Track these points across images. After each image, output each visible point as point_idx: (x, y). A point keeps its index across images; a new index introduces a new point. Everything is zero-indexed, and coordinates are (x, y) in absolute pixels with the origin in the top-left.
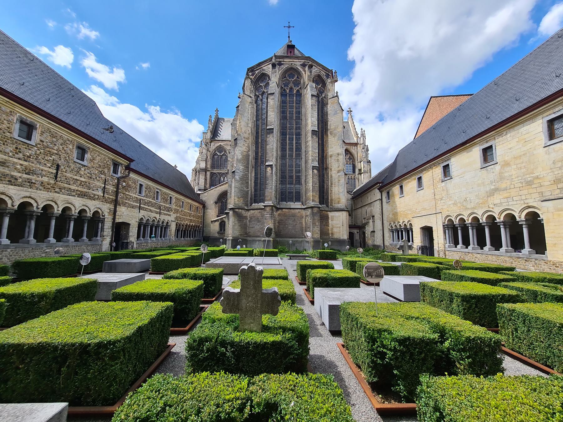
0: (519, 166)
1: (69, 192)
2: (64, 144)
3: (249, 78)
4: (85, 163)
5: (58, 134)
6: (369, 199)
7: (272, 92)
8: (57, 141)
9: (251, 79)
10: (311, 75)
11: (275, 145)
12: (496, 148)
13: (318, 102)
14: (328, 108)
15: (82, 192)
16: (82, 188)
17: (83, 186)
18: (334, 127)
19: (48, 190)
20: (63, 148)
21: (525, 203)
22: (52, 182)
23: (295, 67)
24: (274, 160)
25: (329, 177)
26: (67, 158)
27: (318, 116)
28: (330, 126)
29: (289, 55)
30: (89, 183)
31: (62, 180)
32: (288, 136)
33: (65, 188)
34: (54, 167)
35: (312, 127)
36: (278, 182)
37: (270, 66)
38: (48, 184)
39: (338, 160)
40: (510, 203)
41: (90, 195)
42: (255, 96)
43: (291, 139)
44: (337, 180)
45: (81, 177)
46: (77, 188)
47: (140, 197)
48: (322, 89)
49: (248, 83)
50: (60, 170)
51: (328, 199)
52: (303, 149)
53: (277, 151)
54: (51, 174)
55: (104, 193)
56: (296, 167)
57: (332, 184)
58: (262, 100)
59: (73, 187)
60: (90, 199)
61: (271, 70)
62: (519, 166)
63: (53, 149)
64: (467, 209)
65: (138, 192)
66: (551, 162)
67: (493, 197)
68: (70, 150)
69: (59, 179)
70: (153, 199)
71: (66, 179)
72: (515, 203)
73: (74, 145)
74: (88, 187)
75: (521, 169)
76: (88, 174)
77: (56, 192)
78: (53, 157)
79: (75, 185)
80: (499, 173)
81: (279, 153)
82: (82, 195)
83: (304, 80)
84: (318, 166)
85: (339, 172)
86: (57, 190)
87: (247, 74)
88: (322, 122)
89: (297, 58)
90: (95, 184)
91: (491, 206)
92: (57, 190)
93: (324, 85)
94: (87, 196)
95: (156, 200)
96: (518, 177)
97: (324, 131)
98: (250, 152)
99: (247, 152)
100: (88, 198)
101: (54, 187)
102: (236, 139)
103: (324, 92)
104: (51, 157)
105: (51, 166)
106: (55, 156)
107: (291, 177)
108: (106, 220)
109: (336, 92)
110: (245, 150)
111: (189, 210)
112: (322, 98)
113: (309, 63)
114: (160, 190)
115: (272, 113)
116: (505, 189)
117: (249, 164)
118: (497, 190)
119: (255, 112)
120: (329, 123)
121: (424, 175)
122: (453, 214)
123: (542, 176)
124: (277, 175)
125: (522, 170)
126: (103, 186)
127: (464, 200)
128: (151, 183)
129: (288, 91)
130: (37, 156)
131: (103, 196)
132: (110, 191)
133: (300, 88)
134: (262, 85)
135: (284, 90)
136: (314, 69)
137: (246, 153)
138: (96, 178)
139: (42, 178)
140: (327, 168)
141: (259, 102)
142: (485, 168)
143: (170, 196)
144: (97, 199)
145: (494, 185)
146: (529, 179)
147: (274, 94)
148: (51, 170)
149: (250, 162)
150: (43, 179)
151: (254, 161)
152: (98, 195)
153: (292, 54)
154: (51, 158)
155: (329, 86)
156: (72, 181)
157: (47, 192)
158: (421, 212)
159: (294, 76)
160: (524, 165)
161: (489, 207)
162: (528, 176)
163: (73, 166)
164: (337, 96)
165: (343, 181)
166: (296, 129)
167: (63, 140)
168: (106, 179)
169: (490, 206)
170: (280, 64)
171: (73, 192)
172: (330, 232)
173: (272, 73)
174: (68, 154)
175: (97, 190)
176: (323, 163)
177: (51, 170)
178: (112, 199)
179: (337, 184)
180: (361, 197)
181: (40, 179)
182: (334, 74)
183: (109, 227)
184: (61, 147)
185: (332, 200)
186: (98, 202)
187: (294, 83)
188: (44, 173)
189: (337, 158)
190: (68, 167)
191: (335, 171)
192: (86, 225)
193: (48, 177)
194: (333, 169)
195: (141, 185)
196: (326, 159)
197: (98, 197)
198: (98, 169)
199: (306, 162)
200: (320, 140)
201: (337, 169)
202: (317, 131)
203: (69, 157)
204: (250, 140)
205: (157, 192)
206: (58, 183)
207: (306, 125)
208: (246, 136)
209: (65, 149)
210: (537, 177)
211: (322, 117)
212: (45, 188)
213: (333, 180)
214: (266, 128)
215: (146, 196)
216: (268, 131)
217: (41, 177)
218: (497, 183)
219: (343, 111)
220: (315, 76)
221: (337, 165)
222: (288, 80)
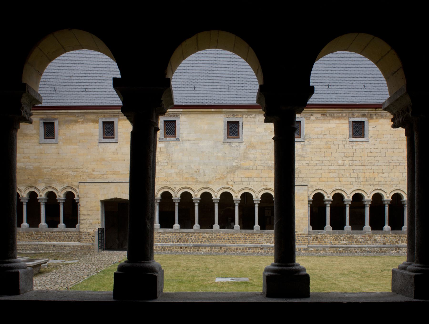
12: (243, 126)
21: (264, 185)
40: (251, 183)
67: (234, 175)
72: (255, 183)
80: (244, 153)
91: (231, 183)
96: (261, 160)
116: (248, 169)
118: (238, 167)
121: (121, 122)
122: (175, 186)
125: (266, 156)
127: (196, 171)
158: (105, 176)
161: (227, 184)
169: (228, 183)
218: (240, 161)
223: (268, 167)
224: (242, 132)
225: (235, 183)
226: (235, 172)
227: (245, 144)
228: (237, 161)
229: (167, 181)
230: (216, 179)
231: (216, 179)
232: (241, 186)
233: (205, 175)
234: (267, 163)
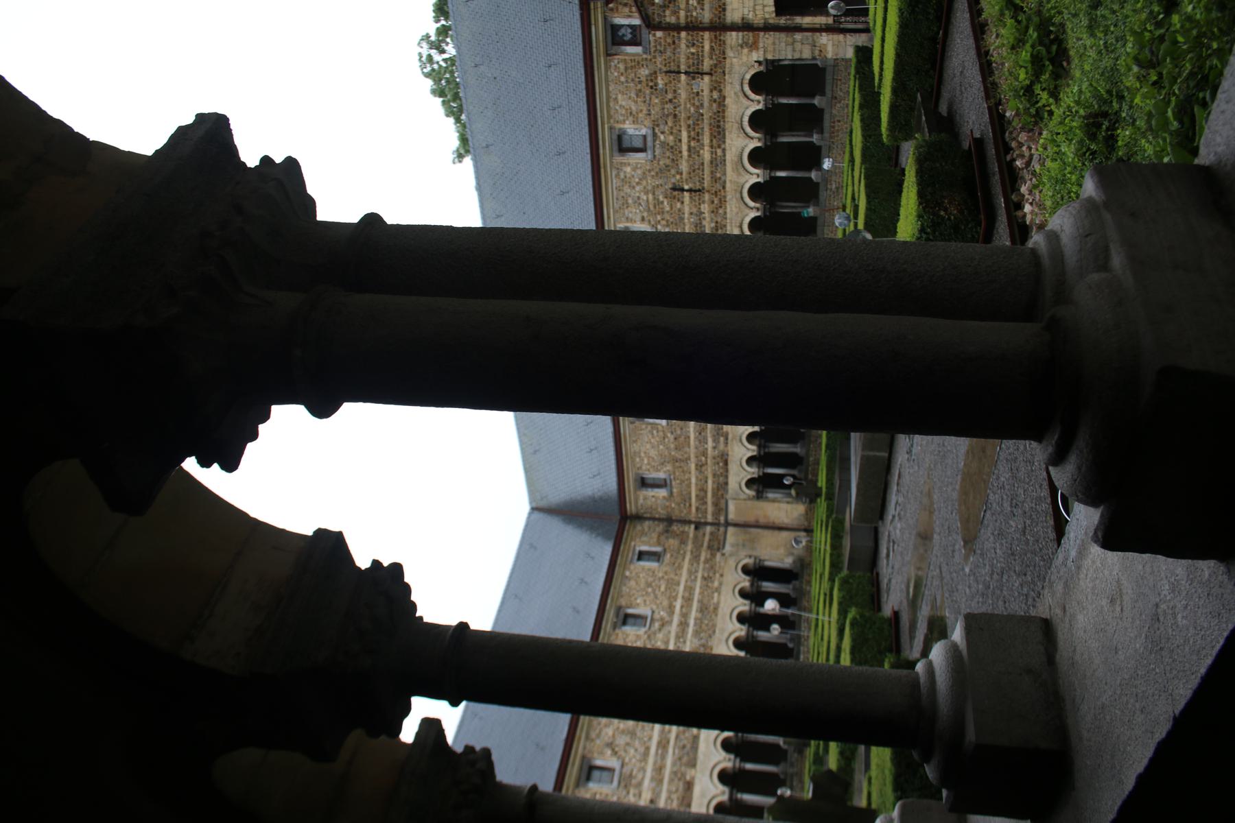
2: (630, 183)
5: (618, 195)
8: (630, 196)
15: (711, 134)
16: (703, 135)
17: (698, 134)
19: (723, 202)
20: (638, 184)
22: (707, 197)
26: (653, 173)
30: (689, 118)
33: (712, 172)
34: (678, 194)
38: (713, 202)
41: (715, 114)
45: (680, 141)
46: (706, 148)
50: (680, 184)
55: (702, 74)
59: (706, 155)
60: (724, 111)
63: (648, 200)
68: (634, 169)
73: (621, 163)
76: (670, 124)
78: (661, 198)
79: (701, 152)
82: (719, 133)
86: (718, 186)
90: (685, 104)
94: (719, 121)
100: (724, 117)
104: (662, 202)
105: (679, 200)
106: (658, 195)
108: (770, 57)
126: (683, 77)
130: (670, 223)
131: (710, 74)
132: (693, 50)
138: (671, 101)
139: (704, 213)
144: (720, 91)
150: (706, 212)
152: (711, 91)
154: (665, 203)
157: (728, 203)
167: (623, 186)
168: (667, 72)
171: (716, 155)
174: (644, 173)
175: (698, 93)
178: (711, 42)
181: (707, 215)
183: (790, 40)
184: (638, 188)
186: (728, 88)
192: (784, 101)
197: (715, 88)
198: (648, 98)
206: (706, 185)
209: (637, 180)
217: (704, 215)
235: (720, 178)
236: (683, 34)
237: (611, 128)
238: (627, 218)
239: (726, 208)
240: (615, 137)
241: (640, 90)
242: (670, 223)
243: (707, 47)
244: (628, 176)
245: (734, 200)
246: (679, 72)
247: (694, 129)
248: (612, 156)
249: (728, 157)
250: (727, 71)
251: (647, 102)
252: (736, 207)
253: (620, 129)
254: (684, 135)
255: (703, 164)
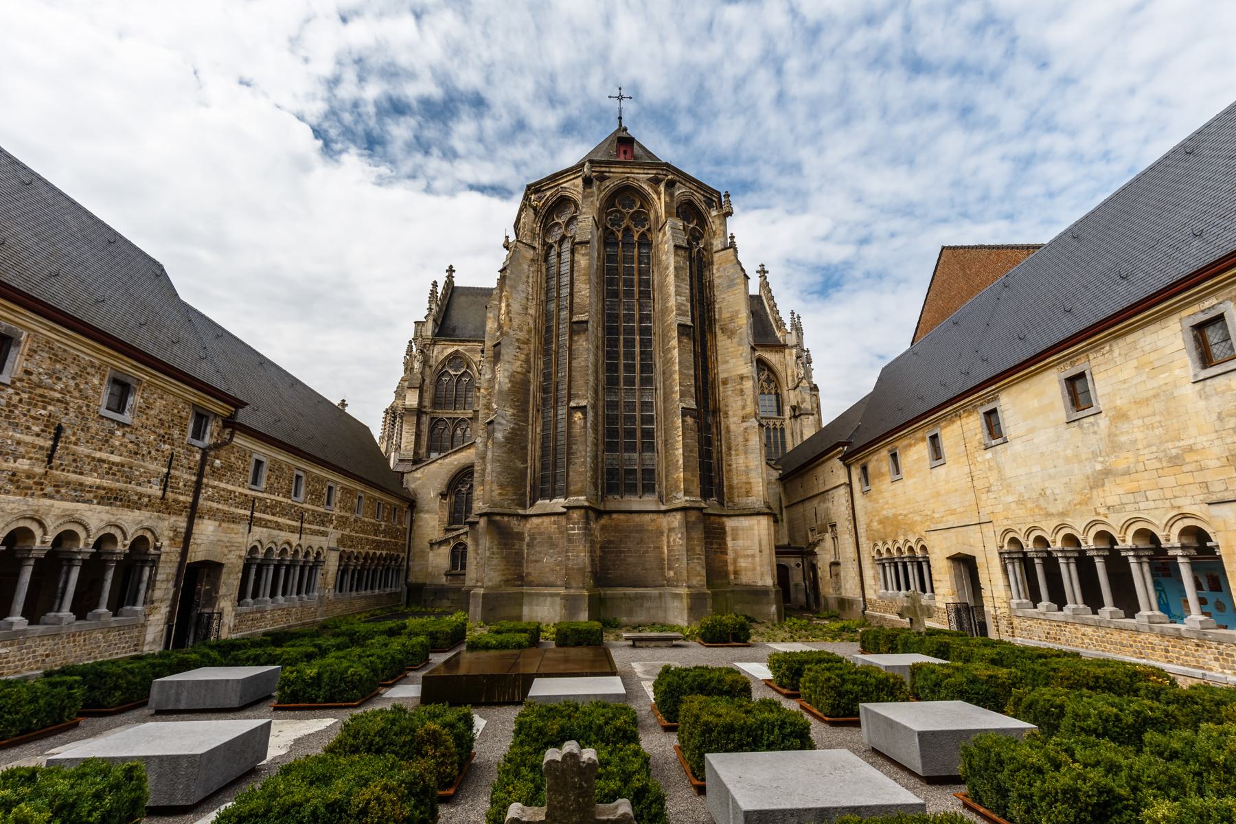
0: (1147, 421)
1: (77, 494)
2: (81, 376)
3: (531, 206)
4: (127, 417)
6: (821, 481)
7: (584, 239)
9: (535, 209)
10: (672, 201)
11: (591, 358)
13: (691, 259)
14: (715, 271)
15: (111, 489)
17: (114, 474)
18: (729, 315)
20: (77, 385)
21: (1173, 507)
22: (39, 470)
23: (635, 184)
24: (590, 394)
25: (723, 433)
26: (84, 408)
27: (691, 289)
28: (720, 313)
29: (622, 158)
30: (131, 468)
31: (65, 463)
32: (621, 337)
33: (68, 483)
34: (50, 433)
35: (679, 318)
36: (601, 447)
37: (579, 182)
38: (28, 477)
39: (742, 391)
40: (1142, 506)
42: (543, 246)
43: (629, 343)
44: (741, 439)
45: (112, 453)
47: (253, 493)
48: (699, 232)
49: (528, 216)
51: (721, 484)
52: (658, 366)
53: (596, 372)
54: (40, 452)
55: (164, 490)
56: (642, 411)
57: (729, 449)
58: (559, 255)
59: (90, 480)
60: (128, 507)
61: (580, 189)
62: (1147, 421)
63: (52, 389)
64: (1049, 515)
65: (250, 479)
66: (1214, 416)
68: (94, 388)
69: (56, 462)
70: (287, 494)
71: (75, 461)
72: (1152, 504)
73: (104, 376)
74: (127, 477)
75: (1153, 428)
76: (130, 445)
77: (45, 495)
78: (50, 408)
79: (96, 475)
80: (1109, 436)
81: (601, 376)
82: (110, 498)
83: (656, 212)
84: (694, 407)
85: (744, 419)
86: (49, 490)
87: (526, 198)
88: (702, 304)
89: (641, 165)
90: (144, 467)
91: (1102, 510)
92: (49, 490)
93: (703, 221)
94: (121, 500)
95: (293, 498)
96: (1150, 446)
97: (707, 323)
98: (531, 375)
99: (525, 374)
100: (123, 506)
101: (42, 484)
102: (499, 344)
103: (702, 236)
104: (44, 408)
105: (43, 431)
106: (54, 405)
107: (631, 433)
108: (162, 558)
109: (729, 235)
110: (519, 370)
111: (374, 518)
112: (699, 251)
113: (667, 175)
114: (305, 471)
115: (583, 286)
116: (1127, 473)
117: (528, 403)
118: (1107, 473)
119: (544, 282)
120: (717, 306)
123: (1199, 446)
124: (597, 430)
125: (1157, 432)
126: (165, 470)
128: (282, 457)
129: (620, 235)
130: (11, 408)
131: (163, 498)
132: (181, 484)
133: (649, 230)
134: (560, 221)
135: (612, 233)
136: (679, 189)
137: (522, 377)
138: (150, 453)
139: (15, 461)
140: (716, 411)
141: (553, 259)
142: (1076, 423)
143: (329, 484)
144: (146, 506)
145: (1102, 463)
146: (1174, 452)
147: (588, 242)
148: (40, 442)
149: (531, 400)
150: (17, 464)
151: (539, 395)
152: (149, 496)
153: (629, 155)
154: (43, 412)
155: (715, 225)
156: (89, 464)
157: (21, 498)
159: (634, 202)
160: (1157, 418)
161: (1098, 514)
162: (1170, 445)
163: (94, 426)
164: (733, 246)
165: (755, 441)
166: (641, 320)
167: (78, 365)
168: (172, 454)
170: (602, 178)
172: (731, 568)
173: (584, 197)
174: (87, 398)
175: (149, 482)
176: (706, 399)
177: (40, 442)
179: (741, 448)
180: (802, 476)
181: (11, 464)
182: (723, 199)
183: (170, 577)
184: (72, 383)
185: (731, 487)
186: (147, 514)
187: (632, 217)
188: (22, 449)
189: (738, 387)
190: (83, 430)
191: (736, 419)
192: (110, 575)
193: (31, 458)
194: (730, 413)
195: (259, 463)
196: (713, 388)
197: (150, 501)
198: (157, 430)
199: (667, 398)
200: (698, 344)
201: (740, 413)
202: (690, 327)
203: (88, 406)
204: (532, 346)
205: (298, 477)
206: (55, 472)
207: (665, 311)
208: (522, 335)
210: (1191, 449)
211: (701, 292)
212: (18, 487)
213: (732, 438)
214: (571, 318)
215: (270, 490)
216: (575, 327)
217: (12, 461)
219: (748, 278)
220: (682, 204)
221: (740, 403)
222: (619, 211)
223: (1171, 458)
224: (1095, 390)
225: (1109, 508)
226: (1103, 485)
227: (1106, 416)
228: (1101, 459)
229: (1007, 519)
230: (1075, 505)
231: (1075, 505)
232: (1123, 514)
233: (1056, 500)
234: (1164, 451)
235: (58, 492)
236: (205, 480)
237: (139, 381)
238: (35, 352)
239: (15, 494)
240: (129, 380)
241: (162, 424)
242: (11, 408)
243: (182, 498)
244: (89, 377)
245: (25, 508)
246: (169, 468)
247: (119, 471)
248: (113, 368)
249: (81, 506)
250: (161, 514)
251: (153, 429)
252: (12, 509)
253: (135, 390)
254: (116, 459)
255: (81, 474)
